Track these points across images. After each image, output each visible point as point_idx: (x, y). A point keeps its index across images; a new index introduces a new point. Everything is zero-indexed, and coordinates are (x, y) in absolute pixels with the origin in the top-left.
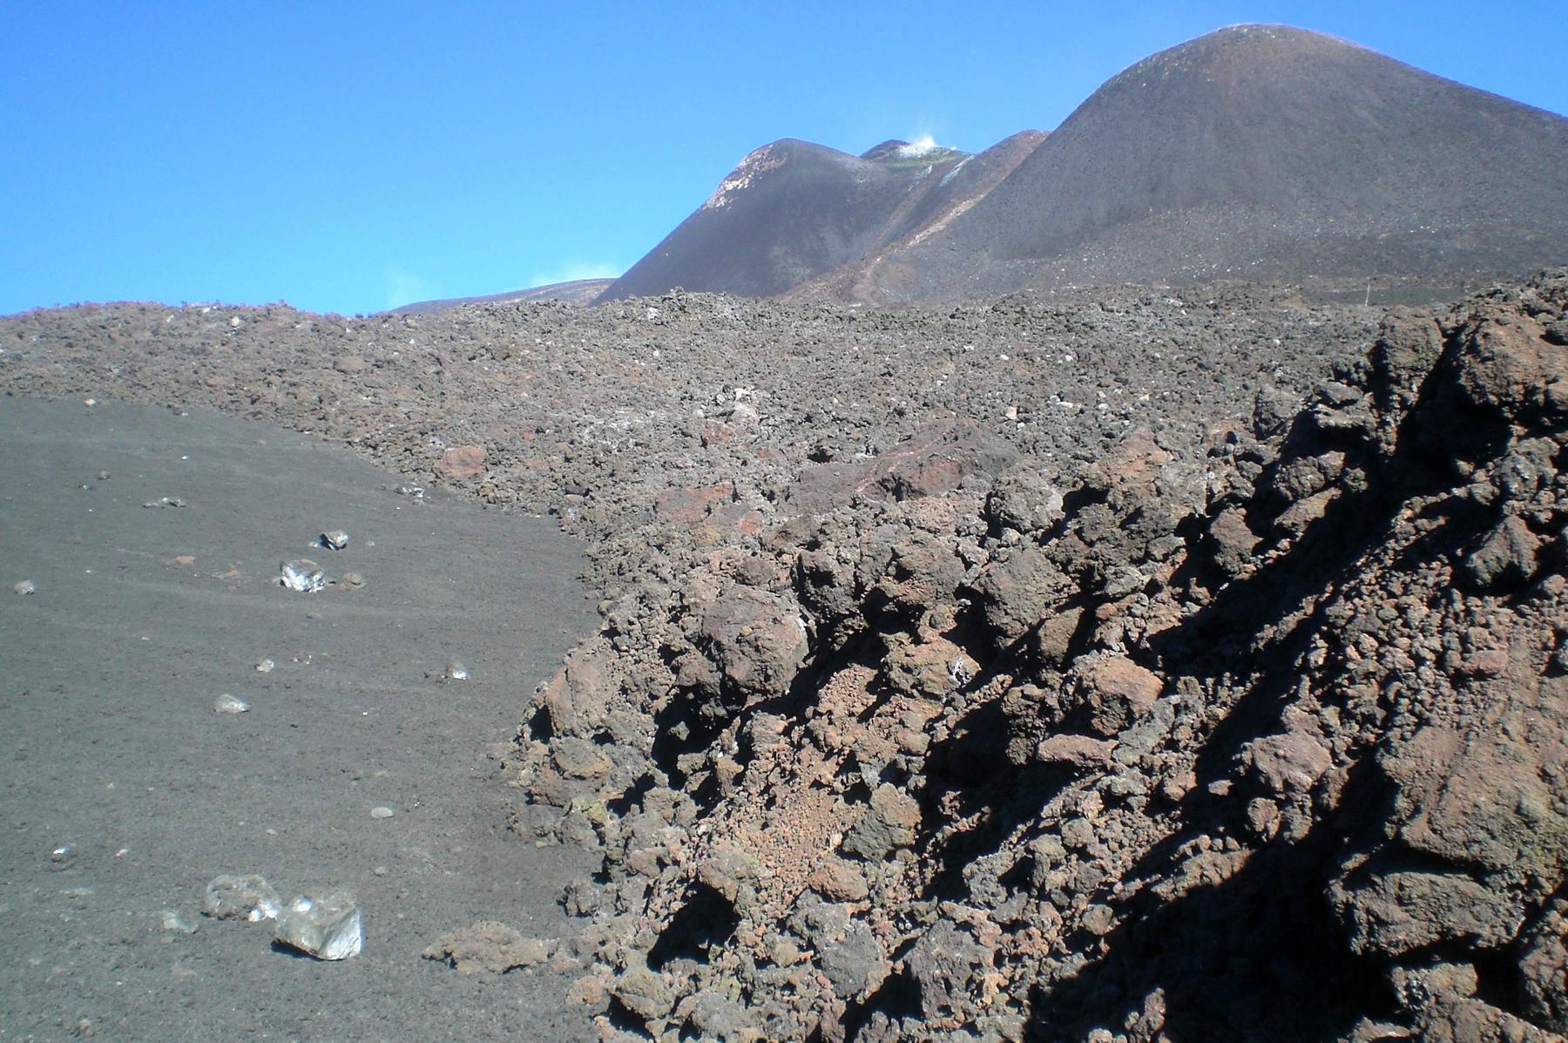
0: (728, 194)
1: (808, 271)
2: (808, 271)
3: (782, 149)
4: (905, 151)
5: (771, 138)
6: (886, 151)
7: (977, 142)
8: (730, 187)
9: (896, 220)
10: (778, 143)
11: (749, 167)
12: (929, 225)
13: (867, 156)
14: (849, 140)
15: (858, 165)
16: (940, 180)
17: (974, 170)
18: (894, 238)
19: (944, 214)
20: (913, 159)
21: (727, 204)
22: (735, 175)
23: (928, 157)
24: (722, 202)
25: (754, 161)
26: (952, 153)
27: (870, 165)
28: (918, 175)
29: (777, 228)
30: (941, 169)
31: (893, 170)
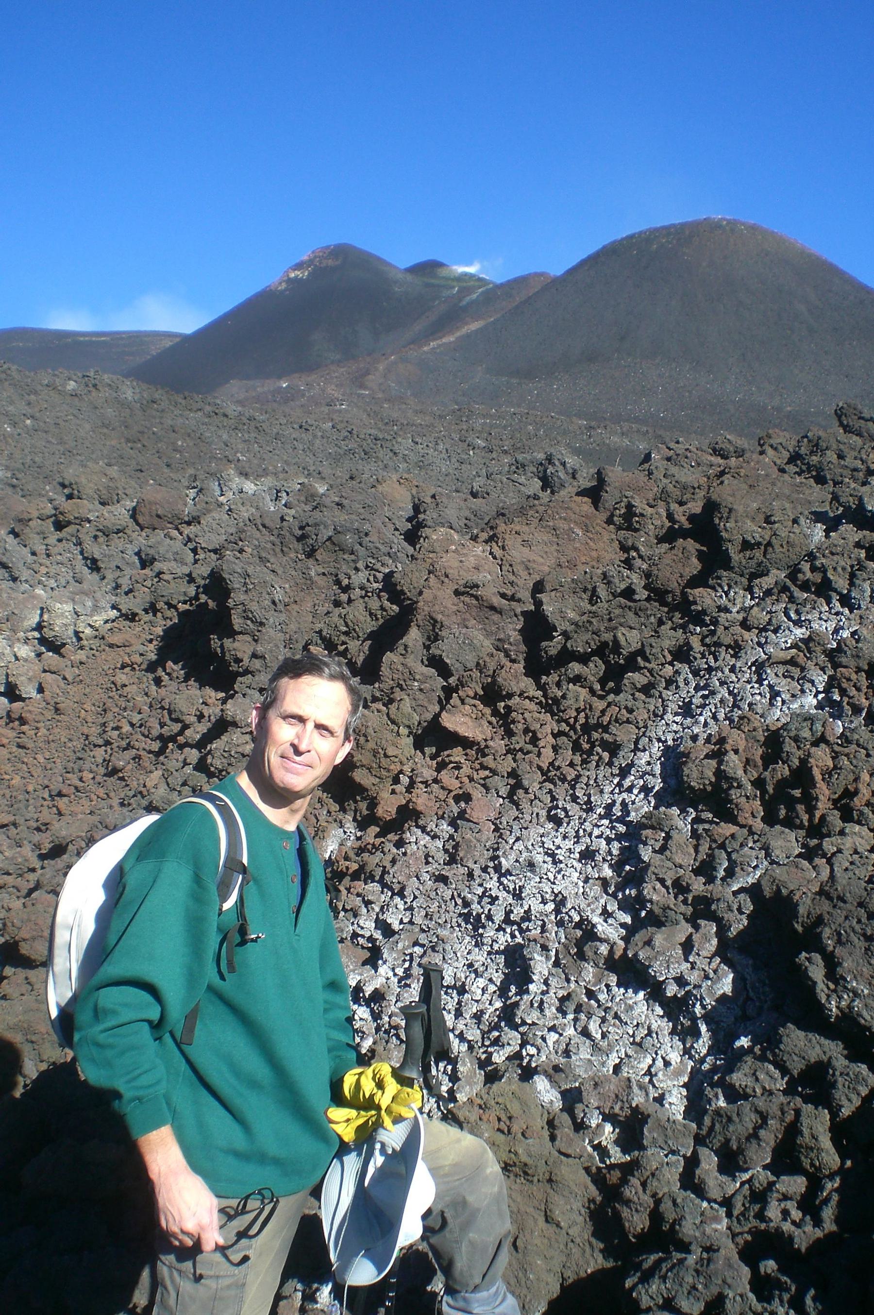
0: (289, 281)
2: (338, 357)
4: (443, 272)
5: (333, 239)
6: (428, 268)
8: (292, 275)
9: (418, 327)
10: (335, 246)
11: (311, 262)
14: (399, 253)
15: (400, 276)
16: (460, 300)
17: (494, 294)
18: (413, 342)
19: (458, 329)
20: (447, 279)
21: (286, 290)
22: (299, 266)
24: (284, 286)
25: (315, 257)
26: (480, 280)
27: (409, 277)
28: (446, 293)
29: (329, 312)
30: (466, 290)
31: (427, 285)
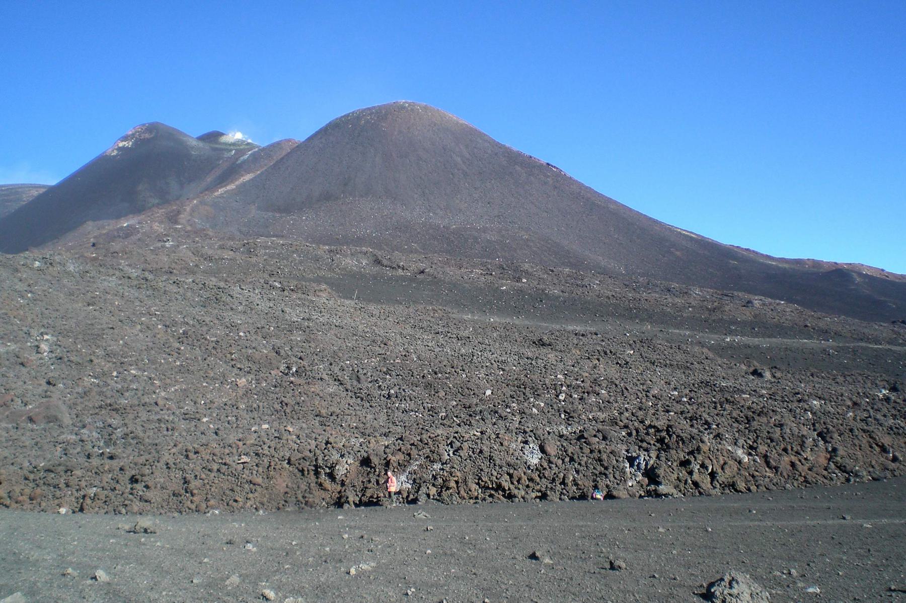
0: (119, 149)
1: (157, 201)
2: (157, 201)
3: (153, 128)
4: (224, 139)
7: (262, 142)
8: (121, 145)
9: (209, 179)
10: (150, 124)
11: (133, 134)
12: (227, 185)
13: (202, 138)
15: (194, 143)
16: (237, 160)
18: (207, 190)
19: (236, 180)
20: (226, 144)
22: (125, 138)
23: (234, 144)
26: (248, 144)
27: (201, 144)
28: (226, 155)
